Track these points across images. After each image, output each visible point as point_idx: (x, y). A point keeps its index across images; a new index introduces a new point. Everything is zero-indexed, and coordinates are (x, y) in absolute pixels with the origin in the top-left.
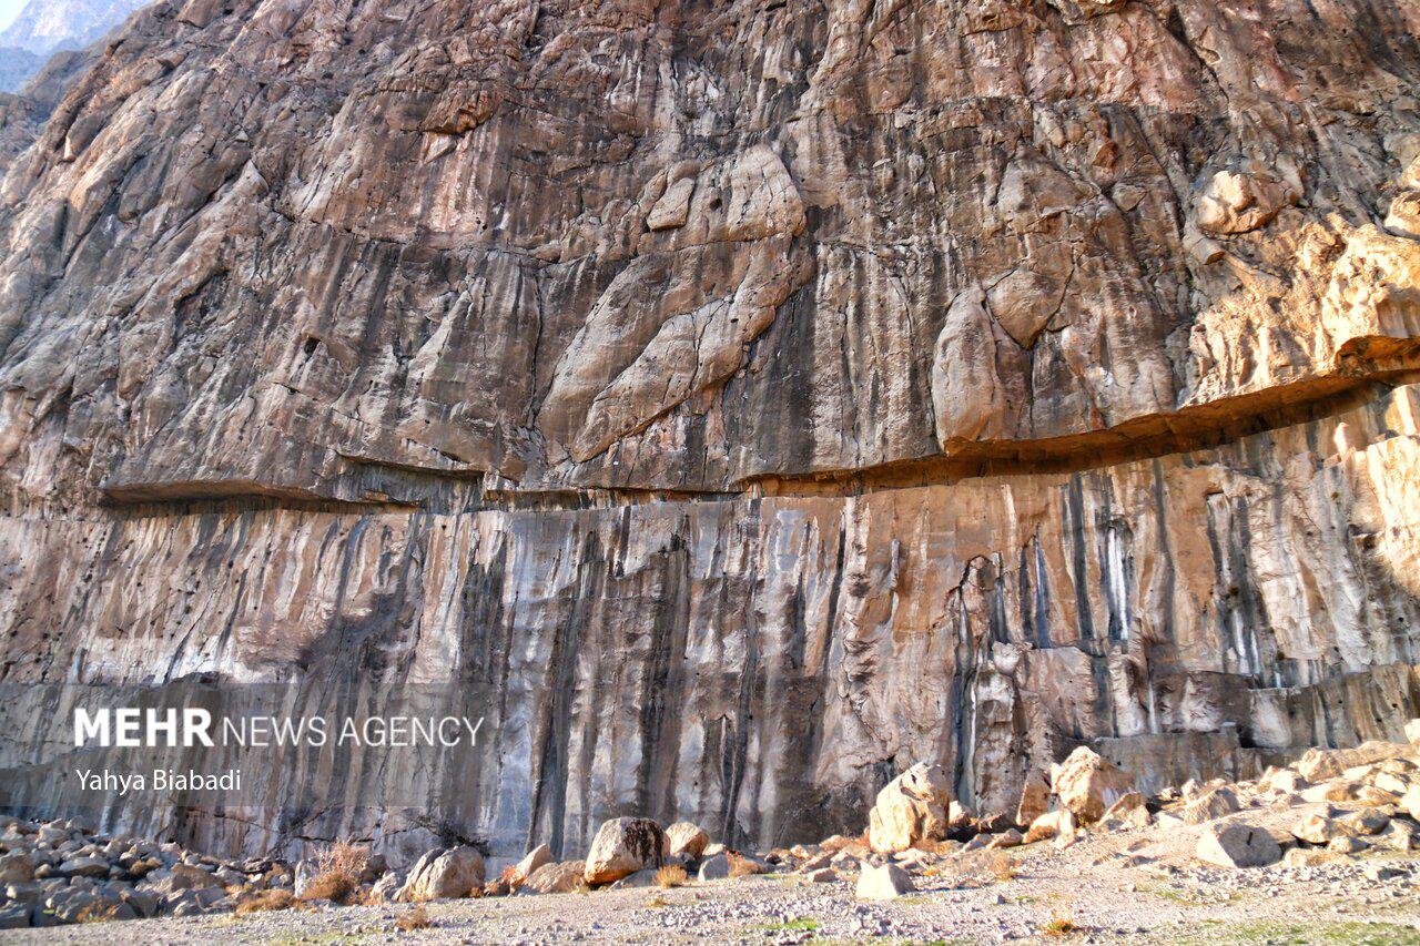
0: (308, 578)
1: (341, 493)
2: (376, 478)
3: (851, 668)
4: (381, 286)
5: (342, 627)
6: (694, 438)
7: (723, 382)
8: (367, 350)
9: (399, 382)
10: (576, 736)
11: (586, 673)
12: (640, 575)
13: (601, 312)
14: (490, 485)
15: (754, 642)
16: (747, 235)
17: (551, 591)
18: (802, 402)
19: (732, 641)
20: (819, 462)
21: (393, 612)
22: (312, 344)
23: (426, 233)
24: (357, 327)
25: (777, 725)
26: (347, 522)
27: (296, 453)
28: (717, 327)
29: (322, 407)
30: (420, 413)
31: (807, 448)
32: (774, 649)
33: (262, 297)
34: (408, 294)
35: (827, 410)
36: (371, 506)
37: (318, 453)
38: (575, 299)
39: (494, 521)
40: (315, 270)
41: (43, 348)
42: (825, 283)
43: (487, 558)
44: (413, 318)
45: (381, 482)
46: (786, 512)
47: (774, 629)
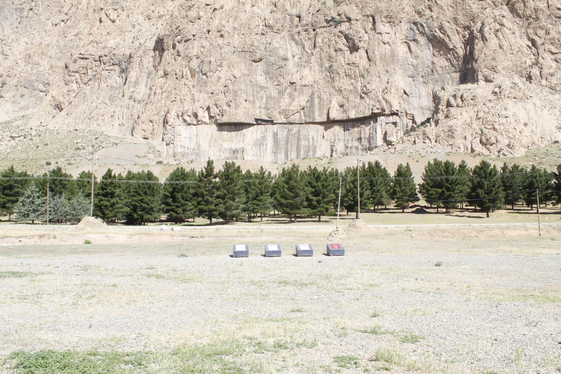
0: (252, 134)
1: (255, 123)
2: (259, 122)
3: (320, 144)
4: (253, 91)
5: (257, 140)
6: (300, 116)
7: (303, 109)
8: (254, 103)
9: (260, 107)
10: (289, 153)
11: (289, 145)
12: (295, 134)
13: (286, 96)
14: (275, 122)
15: (309, 142)
16: (305, 86)
17: (284, 136)
18: (313, 113)
19: (306, 141)
20: (316, 121)
21: (264, 138)
22: (246, 101)
23: (256, 81)
24: (252, 98)
25: (311, 151)
26: (255, 126)
27: (248, 118)
28: (302, 100)
29: (250, 111)
30: (264, 112)
31: (314, 118)
32: (311, 143)
33: (236, 92)
34: (257, 92)
35: (317, 113)
36: (258, 124)
37: (251, 118)
38: (281, 93)
39: (275, 126)
40: (243, 88)
41: (202, 100)
42: (316, 94)
43: (275, 131)
44: (259, 96)
45: (259, 122)
46: (312, 126)
47: (311, 140)
